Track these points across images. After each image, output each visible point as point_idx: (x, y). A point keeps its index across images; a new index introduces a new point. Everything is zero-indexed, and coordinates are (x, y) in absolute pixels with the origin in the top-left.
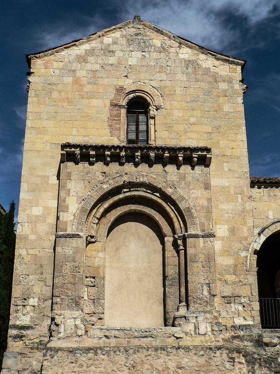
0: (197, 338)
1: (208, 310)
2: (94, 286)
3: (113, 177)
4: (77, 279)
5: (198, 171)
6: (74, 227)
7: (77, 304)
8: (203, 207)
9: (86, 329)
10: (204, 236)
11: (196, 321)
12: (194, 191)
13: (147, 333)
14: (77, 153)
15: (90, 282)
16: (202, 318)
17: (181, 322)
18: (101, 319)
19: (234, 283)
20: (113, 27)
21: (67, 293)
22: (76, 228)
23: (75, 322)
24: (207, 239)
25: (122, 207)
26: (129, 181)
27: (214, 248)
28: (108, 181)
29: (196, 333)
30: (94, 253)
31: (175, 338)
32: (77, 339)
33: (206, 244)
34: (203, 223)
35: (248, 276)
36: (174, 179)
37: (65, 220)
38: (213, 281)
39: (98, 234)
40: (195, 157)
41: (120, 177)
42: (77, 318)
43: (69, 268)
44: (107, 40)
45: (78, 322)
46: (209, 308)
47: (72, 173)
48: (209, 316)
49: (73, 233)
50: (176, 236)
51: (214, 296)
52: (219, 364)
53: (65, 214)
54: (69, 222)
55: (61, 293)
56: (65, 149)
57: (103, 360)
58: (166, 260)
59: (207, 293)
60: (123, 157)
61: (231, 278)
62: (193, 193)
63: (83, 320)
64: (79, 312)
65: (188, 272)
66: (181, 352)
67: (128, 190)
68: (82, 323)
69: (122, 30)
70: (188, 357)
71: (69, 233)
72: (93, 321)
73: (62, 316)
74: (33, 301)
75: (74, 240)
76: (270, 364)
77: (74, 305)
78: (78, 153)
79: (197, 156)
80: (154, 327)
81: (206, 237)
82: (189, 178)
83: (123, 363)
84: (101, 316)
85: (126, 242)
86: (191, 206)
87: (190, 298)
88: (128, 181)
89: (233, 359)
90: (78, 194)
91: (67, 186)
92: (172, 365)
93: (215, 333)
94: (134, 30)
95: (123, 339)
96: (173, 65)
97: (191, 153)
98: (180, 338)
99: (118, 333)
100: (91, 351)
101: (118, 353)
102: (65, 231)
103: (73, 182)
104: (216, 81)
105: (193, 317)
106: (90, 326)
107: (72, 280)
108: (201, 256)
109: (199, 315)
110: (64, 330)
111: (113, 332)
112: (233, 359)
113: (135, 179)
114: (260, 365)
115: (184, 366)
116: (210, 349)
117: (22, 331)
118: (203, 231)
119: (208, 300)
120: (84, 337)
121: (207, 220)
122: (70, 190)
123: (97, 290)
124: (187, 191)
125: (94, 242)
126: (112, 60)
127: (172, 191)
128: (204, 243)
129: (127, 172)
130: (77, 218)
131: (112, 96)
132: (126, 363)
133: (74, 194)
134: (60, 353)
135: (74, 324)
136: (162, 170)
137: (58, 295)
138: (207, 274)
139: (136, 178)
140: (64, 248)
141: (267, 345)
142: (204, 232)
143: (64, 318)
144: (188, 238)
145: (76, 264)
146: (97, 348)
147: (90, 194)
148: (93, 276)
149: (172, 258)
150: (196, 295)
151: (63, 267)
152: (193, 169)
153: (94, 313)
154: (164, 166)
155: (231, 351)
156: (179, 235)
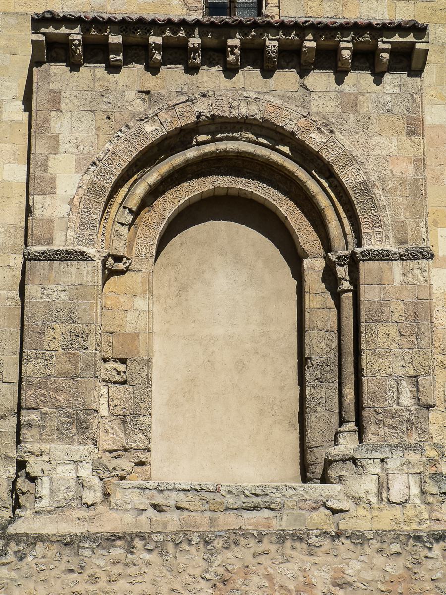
0: (384, 511)
1: (412, 441)
2: (124, 383)
3: (171, 103)
4: (80, 365)
5: (392, 86)
6: (72, 234)
7: (83, 427)
8: (402, 182)
10: (405, 255)
11: (382, 469)
12: (378, 138)
13: (259, 499)
14: (74, 40)
15: (115, 373)
16: (398, 462)
17: (344, 473)
18: (141, 463)
21: (57, 400)
22: (76, 236)
23: (77, 471)
25: (194, 183)
26: (212, 113)
27: (430, 287)
28: (156, 115)
29: (382, 499)
30: (123, 299)
31: (328, 512)
32: (83, 513)
33: (410, 275)
34: (403, 222)
36: (327, 110)
37: (47, 214)
38: (426, 369)
39: (134, 252)
40: (384, 50)
41: (188, 103)
42: (81, 461)
43: (59, 337)
45: (85, 472)
46: (414, 438)
47: (62, 92)
48: (413, 456)
49: (70, 248)
50: (333, 257)
51: (428, 407)
52: (438, 575)
53: (48, 199)
55: (41, 400)
56: (43, 30)
57: (148, 564)
58: (307, 316)
59: (409, 399)
60: (195, 50)
62: (376, 145)
63: (98, 467)
64: (87, 446)
65: (363, 347)
67: (209, 137)
68: (95, 473)
70: (362, 558)
71: (58, 249)
72: (123, 470)
73: (45, 458)
75: (73, 268)
77: (74, 430)
78: (78, 40)
79: (388, 46)
80: (277, 485)
81: (411, 259)
82: (367, 106)
83: (197, 572)
84: (143, 456)
85: (204, 272)
86: (372, 179)
87: (366, 413)
88: (208, 115)
90: (81, 148)
91: (52, 126)
92: (321, 577)
93: (431, 499)
95: (199, 514)
97: (374, 39)
98: (342, 511)
99: (186, 499)
100: (119, 543)
101: (185, 546)
102: (49, 244)
103: (66, 118)
105: (376, 460)
106: (115, 481)
107: (68, 367)
108: (396, 307)
109: (390, 455)
110: (51, 491)
111: (174, 495)
113: (226, 108)
115: (350, 579)
116: (418, 538)
118: (403, 242)
119: (413, 417)
120: (100, 508)
121: (412, 214)
122: (58, 137)
123: (131, 391)
124: (362, 140)
125: (122, 272)
127: (324, 141)
128: (404, 275)
129: (206, 90)
130: (80, 211)
132: (207, 571)
133: (70, 148)
134: (40, 548)
135: (74, 476)
136: (298, 85)
137: (34, 406)
138: (411, 351)
139: (230, 107)
140: (45, 286)
142: (405, 246)
143: (49, 462)
144: (364, 261)
145: (77, 327)
146: (133, 536)
147: (110, 148)
148: (121, 356)
149: (322, 313)
150: (382, 405)
151: (45, 333)
152: (378, 82)
153: (126, 450)
154: (303, 73)
156: (340, 253)
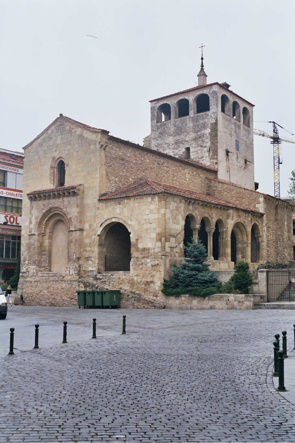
19: (89, 251)
24: (76, 232)
32: (34, 277)
35: (95, 248)
45: (35, 271)
54: (33, 229)
66: (63, 282)
74: (27, 262)
89: (79, 285)
92: (60, 287)
94: (59, 123)
104: (90, 145)
107: (33, 253)
112: (79, 285)
126: (51, 143)
134: (28, 283)
141: (98, 279)
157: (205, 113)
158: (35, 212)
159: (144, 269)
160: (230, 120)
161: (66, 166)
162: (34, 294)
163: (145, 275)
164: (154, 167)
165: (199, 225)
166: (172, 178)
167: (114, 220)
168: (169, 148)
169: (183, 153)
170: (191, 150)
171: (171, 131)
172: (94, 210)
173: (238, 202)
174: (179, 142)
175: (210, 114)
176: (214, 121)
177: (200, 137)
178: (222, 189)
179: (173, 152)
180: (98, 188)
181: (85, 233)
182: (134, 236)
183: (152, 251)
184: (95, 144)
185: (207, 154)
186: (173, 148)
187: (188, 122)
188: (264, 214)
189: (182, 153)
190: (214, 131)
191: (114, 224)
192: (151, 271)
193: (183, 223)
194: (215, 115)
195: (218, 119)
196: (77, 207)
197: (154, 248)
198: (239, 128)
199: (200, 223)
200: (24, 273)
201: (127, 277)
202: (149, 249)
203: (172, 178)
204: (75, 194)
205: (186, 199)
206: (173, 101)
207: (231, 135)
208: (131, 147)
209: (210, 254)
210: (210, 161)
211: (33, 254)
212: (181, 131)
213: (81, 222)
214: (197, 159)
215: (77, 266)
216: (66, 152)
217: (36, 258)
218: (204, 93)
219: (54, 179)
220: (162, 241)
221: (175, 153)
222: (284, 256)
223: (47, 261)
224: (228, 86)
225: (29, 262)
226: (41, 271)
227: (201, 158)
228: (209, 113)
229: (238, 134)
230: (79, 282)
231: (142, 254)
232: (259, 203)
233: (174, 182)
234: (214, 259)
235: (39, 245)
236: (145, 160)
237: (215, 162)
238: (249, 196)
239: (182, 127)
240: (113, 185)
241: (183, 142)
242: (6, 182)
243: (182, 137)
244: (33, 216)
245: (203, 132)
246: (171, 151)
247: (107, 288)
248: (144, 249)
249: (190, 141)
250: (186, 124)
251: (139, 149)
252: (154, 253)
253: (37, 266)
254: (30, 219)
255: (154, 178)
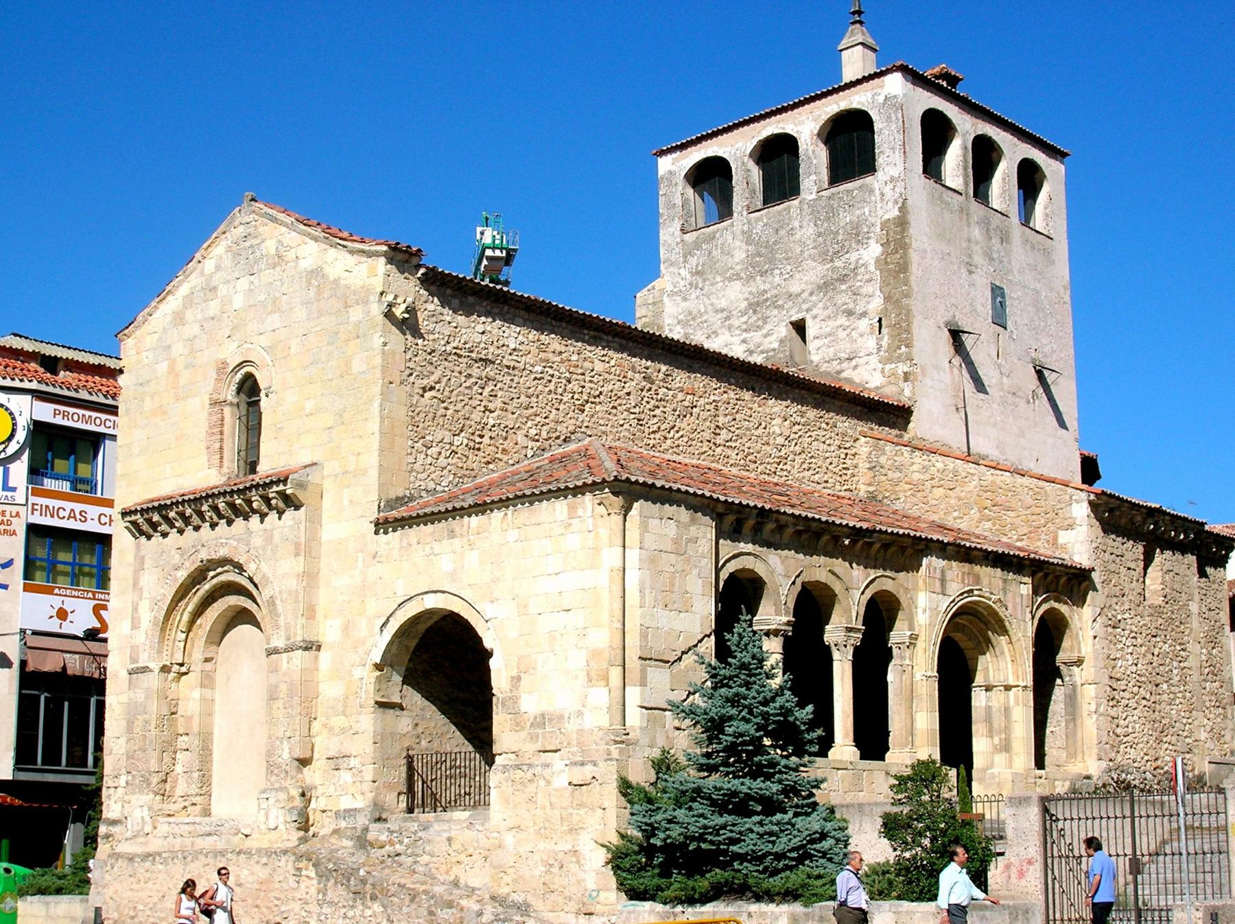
9: (153, 823)
19: (343, 731)
20: (214, 235)
32: (143, 840)
35: (361, 718)
44: (209, 265)
45: (146, 812)
57: (160, 872)
61: (338, 722)
69: (227, 234)
76: (349, 880)
93: (288, 825)
94: (241, 229)
96: (291, 290)
104: (347, 306)
112: (299, 869)
114: (336, 883)
117: (111, 828)
126: (214, 307)
131: (210, 388)
155: (300, 858)
157: (858, 183)
158: (149, 580)
159: (541, 800)
160: (961, 210)
161: (262, 394)
162: (140, 907)
163: (547, 824)
164: (629, 394)
165: (787, 614)
166: (707, 435)
167: (432, 602)
168: (730, 328)
169: (781, 342)
170: (810, 332)
171: (737, 259)
172: (360, 563)
173: (988, 525)
174: (767, 300)
175: (876, 186)
176: (896, 213)
177: (843, 279)
178: (928, 476)
179: (744, 341)
180: (374, 474)
181: (324, 655)
182: (506, 666)
183: (571, 727)
184: (366, 302)
185: (871, 343)
186: (744, 327)
187: (796, 224)
188: (1093, 569)
189: (776, 345)
190: (897, 252)
191: (435, 618)
192: (570, 810)
193: (705, 609)
194: (898, 190)
195: (909, 202)
196: (297, 555)
197: (580, 714)
198: (1005, 238)
199: (791, 605)
200: (114, 822)
201: (481, 836)
202: (561, 717)
203: (707, 435)
204: (291, 502)
205: (720, 509)
206: (740, 145)
207: (970, 269)
208: (523, 313)
209: (846, 735)
210: (883, 371)
211: (140, 749)
212: (771, 261)
213: (310, 612)
214: (835, 363)
215: (295, 792)
216: (264, 341)
217: (154, 765)
218: (855, 105)
219: (221, 448)
220: (611, 685)
221: (753, 348)
222: (1188, 740)
223: (196, 775)
224: (954, 81)
225: (130, 778)
226: (169, 815)
227: (850, 359)
228: (875, 182)
229: (1001, 262)
230: (300, 858)
231: (533, 738)
232: (1070, 527)
233: (719, 450)
234: (862, 758)
235: (165, 711)
236: (587, 365)
237: (900, 372)
238: (1029, 501)
239: (775, 243)
240: (442, 461)
241: (780, 303)
242: (99, 478)
243: (777, 279)
244: (146, 594)
245: (853, 256)
246: (737, 340)
247: (403, 881)
248: (541, 721)
249: (805, 295)
250: (791, 232)
251: (561, 320)
252: (580, 732)
253: (156, 794)
254: (135, 609)
255: (627, 434)
